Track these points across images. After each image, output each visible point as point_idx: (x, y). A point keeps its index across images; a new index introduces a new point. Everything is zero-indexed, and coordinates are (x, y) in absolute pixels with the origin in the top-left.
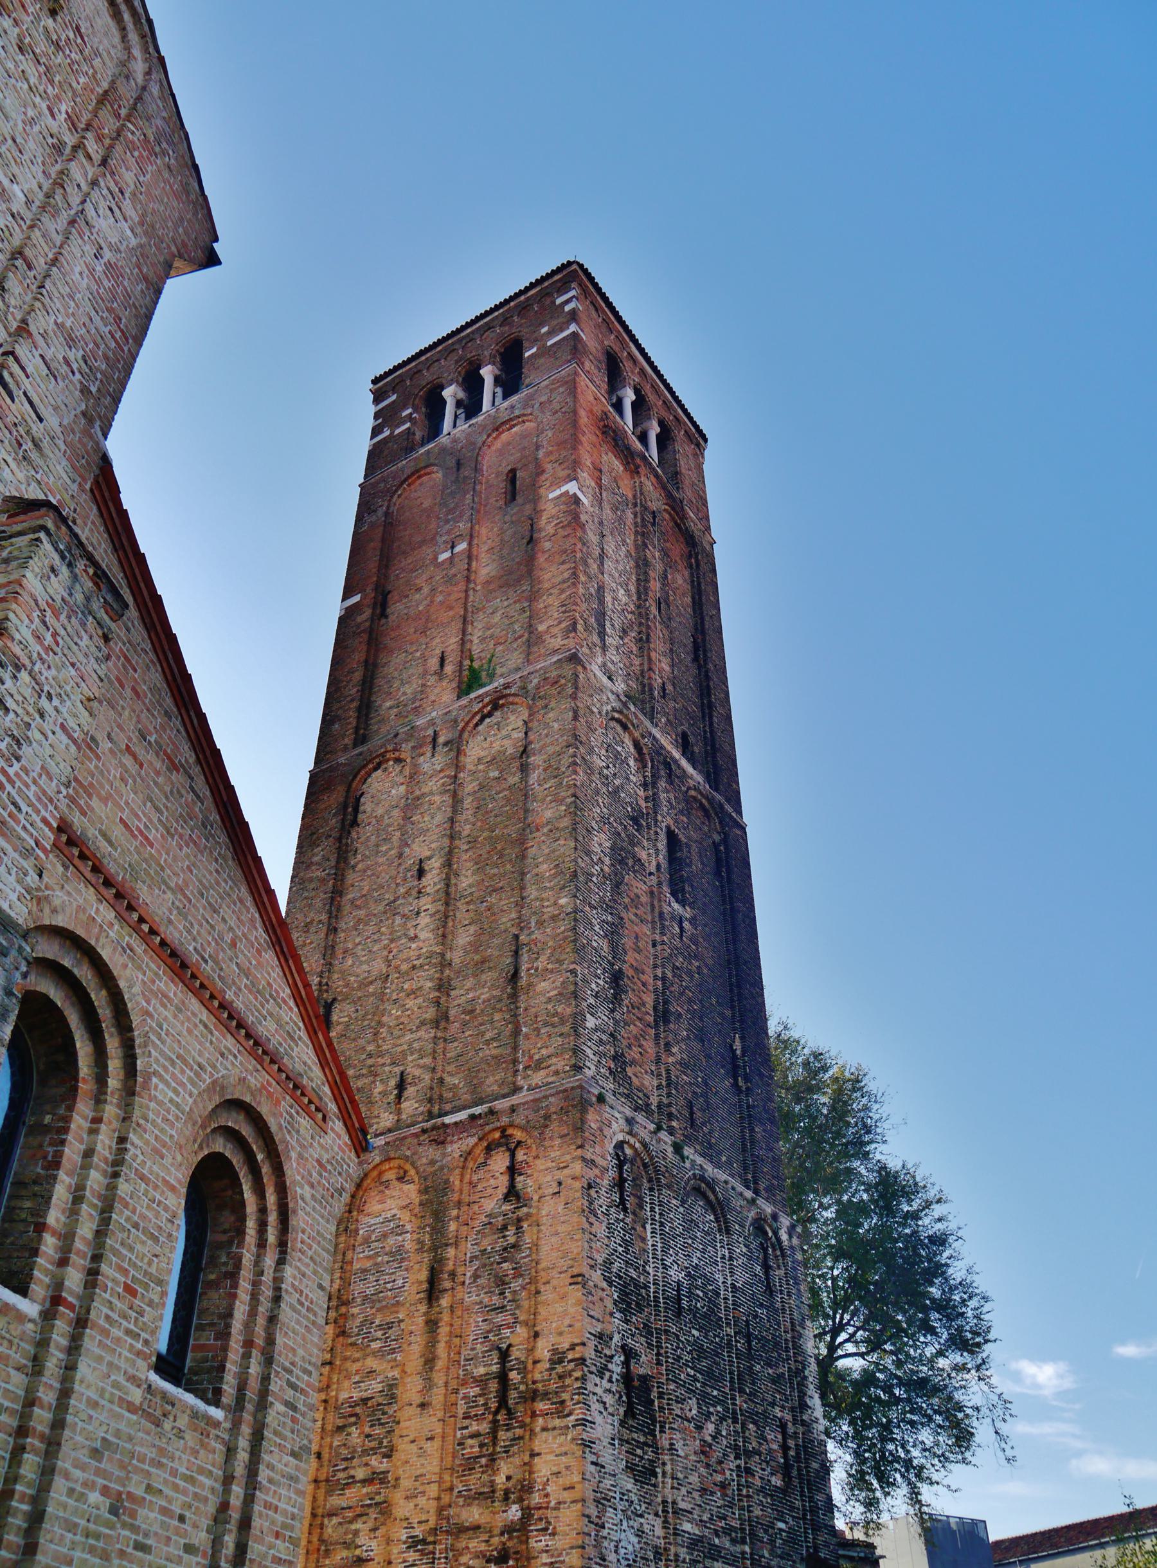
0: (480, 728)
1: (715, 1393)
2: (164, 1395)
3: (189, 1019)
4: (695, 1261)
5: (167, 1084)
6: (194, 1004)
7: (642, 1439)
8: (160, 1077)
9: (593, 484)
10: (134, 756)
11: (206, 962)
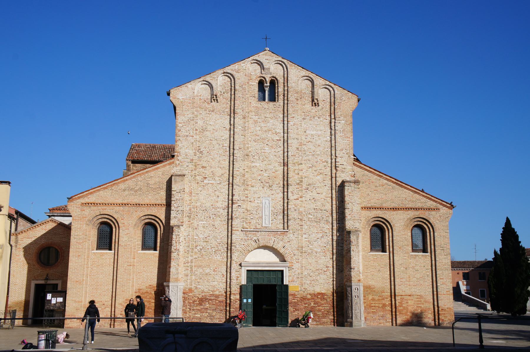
2: (415, 255)
3: (399, 214)
5: (398, 224)
6: (400, 212)
8: (396, 224)
10: (376, 190)
11: (400, 205)
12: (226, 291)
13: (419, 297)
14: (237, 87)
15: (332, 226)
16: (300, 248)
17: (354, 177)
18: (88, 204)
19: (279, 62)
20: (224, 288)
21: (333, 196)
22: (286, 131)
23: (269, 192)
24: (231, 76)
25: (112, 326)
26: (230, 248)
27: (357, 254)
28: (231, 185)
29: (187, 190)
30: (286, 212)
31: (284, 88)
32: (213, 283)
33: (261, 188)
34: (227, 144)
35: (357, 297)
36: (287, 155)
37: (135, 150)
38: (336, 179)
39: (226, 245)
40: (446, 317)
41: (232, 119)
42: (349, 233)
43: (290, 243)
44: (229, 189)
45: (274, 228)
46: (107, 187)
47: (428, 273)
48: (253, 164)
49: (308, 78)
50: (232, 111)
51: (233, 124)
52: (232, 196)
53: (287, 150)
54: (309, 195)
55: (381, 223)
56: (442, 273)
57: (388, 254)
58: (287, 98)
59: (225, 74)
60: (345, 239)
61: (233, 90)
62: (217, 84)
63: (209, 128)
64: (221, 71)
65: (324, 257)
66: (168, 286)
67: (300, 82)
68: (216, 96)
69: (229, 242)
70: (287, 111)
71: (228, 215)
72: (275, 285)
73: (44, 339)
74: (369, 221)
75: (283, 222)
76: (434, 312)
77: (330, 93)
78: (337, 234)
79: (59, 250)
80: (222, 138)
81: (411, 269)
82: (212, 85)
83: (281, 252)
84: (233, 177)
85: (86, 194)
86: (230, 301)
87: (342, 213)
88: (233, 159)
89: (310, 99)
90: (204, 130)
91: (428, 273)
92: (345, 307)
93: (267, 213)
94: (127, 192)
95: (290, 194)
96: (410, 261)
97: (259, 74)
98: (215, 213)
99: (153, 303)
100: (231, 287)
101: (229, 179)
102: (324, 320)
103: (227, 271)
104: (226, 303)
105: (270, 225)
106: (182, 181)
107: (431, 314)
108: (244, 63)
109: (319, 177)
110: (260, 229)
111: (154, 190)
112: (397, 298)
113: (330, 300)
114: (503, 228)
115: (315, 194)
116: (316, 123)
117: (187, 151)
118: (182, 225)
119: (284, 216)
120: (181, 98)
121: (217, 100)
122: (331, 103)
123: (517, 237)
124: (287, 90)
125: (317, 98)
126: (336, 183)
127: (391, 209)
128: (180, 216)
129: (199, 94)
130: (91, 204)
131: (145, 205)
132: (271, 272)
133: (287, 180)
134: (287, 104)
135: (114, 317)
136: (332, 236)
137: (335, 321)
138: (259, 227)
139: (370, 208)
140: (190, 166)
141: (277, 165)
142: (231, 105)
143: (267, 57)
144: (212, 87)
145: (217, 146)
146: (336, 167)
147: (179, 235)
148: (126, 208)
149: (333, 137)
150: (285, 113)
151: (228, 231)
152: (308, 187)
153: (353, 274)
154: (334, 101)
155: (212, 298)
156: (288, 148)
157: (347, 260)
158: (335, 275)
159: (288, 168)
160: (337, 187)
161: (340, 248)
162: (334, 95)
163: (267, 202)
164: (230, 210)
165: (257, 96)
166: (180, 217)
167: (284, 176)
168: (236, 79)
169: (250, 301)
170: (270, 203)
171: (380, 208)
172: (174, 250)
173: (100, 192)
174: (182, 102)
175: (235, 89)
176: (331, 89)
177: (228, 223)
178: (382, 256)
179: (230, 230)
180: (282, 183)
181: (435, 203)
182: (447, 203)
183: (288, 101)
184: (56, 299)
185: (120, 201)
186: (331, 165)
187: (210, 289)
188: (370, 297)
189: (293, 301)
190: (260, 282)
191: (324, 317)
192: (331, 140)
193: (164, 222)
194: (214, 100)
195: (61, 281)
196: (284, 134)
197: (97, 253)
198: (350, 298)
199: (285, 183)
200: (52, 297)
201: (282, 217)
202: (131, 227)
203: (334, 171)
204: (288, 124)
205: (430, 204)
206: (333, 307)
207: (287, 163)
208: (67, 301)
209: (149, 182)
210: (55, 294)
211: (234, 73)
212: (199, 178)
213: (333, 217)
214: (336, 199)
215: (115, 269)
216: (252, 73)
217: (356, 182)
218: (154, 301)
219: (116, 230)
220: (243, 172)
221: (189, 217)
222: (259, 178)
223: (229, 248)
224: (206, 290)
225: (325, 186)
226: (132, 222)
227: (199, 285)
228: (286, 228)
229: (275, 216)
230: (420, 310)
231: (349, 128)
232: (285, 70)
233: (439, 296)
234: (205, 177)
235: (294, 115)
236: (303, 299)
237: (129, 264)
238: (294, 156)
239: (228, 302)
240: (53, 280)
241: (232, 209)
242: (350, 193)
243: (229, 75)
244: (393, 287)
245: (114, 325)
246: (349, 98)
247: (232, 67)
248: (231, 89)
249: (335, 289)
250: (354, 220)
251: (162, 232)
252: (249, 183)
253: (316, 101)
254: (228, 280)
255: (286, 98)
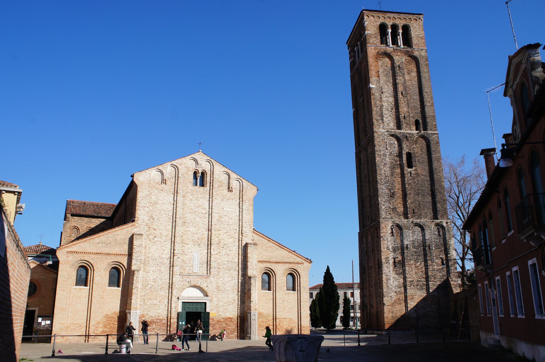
0: (369, 145)
1: (420, 258)
4: (415, 238)
7: (399, 269)
9: (376, 78)
12: (168, 316)
13: (289, 319)
14: (180, 175)
15: (239, 273)
16: (218, 287)
17: (253, 241)
18: (72, 252)
19: (208, 160)
20: (166, 315)
21: (240, 253)
22: (211, 208)
23: (198, 249)
24: (176, 168)
25: (87, 342)
26: (171, 286)
27: (255, 292)
28: (173, 243)
29: (143, 245)
30: (209, 263)
31: (211, 178)
32: (159, 311)
33: (193, 246)
34: (171, 214)
35: (254, 320)
36: (211, 223)
37: (71, 205)
38: (242, 242)
39: (168, 284)
40: (305, 331)
41: (175, 197)
42: (250, 278)
43: (211, 284)
44: (171, 245)
45: (200, 273)
46: (86, 240)
47: (295, 304)
48: (188, 229)
49: (227, 173)
50: (176, 191)
51: (176, 201)
52: (174, 251)
53: (211, 220)
54: (223, 252)
55: (269, 272)
56: (304, 304)
57: (272, 292)
58: (213, 185)
59: (172, 166)
60: (246, 281)
61: (177, 177)
62: (166, 172)
63: (160, 202)
64: (170, 163)
65: (232, 294)
66: (130, 313)
67: (221, 175)
68: (165, 180)
69: (171, 282)
70: (212, 194)
71: (170, 263)
72: (201, 313)
73: (125, 347)
74: (262, 270)
75: (206, 270)
76: (298, 329)
77: (240, 184)
78: (241, 278)
79: (37, 284)
80: (169, 210)
81: (286, 302)
82: (163, 172)
83: (205, 290)
84: (175, 237)
85: (71, 245)
86: (170, 323)
87: (245, 264)
88: (175, 225)
89: (227, 187)
90: (156, 203)
91: (295, 304)
92: (245, 327)
93: (197, 263)
94: (100, 245)
95: (212, 251)
96: (285, 296)
97: (194, 168)
98: (161, 262)
99: (116, 324)
100: (171, 313)
101: (172, 238)
102: (231, 335)
103: (168, 303)
104: (167, 324)
105: (198, 272)
106: (141, 239)
107: (296, 330)
108: (185, 159)
109: (231, 240)
110: (191, 274)
111: (120, 244)
112: (277, 320)
113: (235, 322)
114: (325, 273)
115: (228, 251)
116: (230, 203)
117: (144, 217)
118: (140, 270)
119: (207, 265)
120: (141, 180)
121: (166, 183)
122: (240, 191)
123: (333, 278)
124: (213, 180)
125: (231, 186)
126: (242, 244)
127: (275, 262)
128: (138, 263)
129: (154, 178)
130: (74, 252)
131: (113, 254)
132: (190, 303)
133: (211, 241)
134: (212, 189)
135: (88, 335)
136: (238, 279)
137: (239, 336)
138: (191, 272)
139: (262, 262)
140: (146, 228)
141: (204, 230)
142: (175, 187)
143: (200, 157)
144: (163, 174)
145: (164, 215)
146: (242, 233)
147: (138, 277)
148: (100, 256)
149: (241, 213)
150: (211, 195)
151: (170, 275)
152: (224, 246)
153: (252, 305)
154: (242, 189)
155: (158, 321)
156: (211, 219)
157: (248, 296)
158: (239, 306)
159: (211, 233)
160: (242, 247)
161: (243, 288)
162: (243, 185)
163: (197, 255)
164: (172, 260)
165: (192, 182)
166: (139, 264)
167: (208, 238)
168: (179, 170)
169: (184, 323)
170: (199, 256)
171: (269, 262)
172: (134, 287)
173: (81, 244)
174: (142, 183)
175: (178, 177)
176: (241, 181)
177: (170, 269)
178: (269, 293)
179: (171, 274)
180: (207, 243)
181: (301, 260)
182: (305, 258)
183: (213, 187)
184: (45, 322)
185: (95, 251)
186: (239, 232)
187: (157, 315)
188: (261, 320)
189: (212, 323)
190: (191, 310)
191: (231, 333)
192: (239, 215)
193: (126, 267)
194: (164, 183)
195: (38, 308)
196: (209, 209)
197: (76, 288)
198: (249, 321)
199: (209, 243)
200: (42, 320)
201: (206, 266)
202: (103, 270)
203: (241, 236)
204: (212, 203)
205: (299, 260)
206: (238, 327)
207: (211, 229)
208: (53, 323)
209: (117, 238)
210: (44, 318)
211: (178, 165)
212: (151, 237)
213: (239, 267)
214: (241, 255)
215: (90, 300)
216: (190, 166)
217: (255, 244)
218: (117, 323)
219: (91, 272)
220: (181, 234)
221: (144, 264)
222: (192, 238)
223: (170, 286)
224: (154, 315)
225: (235, 246)
226: (103, 266)
227: (149, 312)
228: (209, 273)
229: (201, 265)
230: (290, 328)
231: (251, 208)
232: (212, 166)
233: (302, 318)
234: (155, 236)
235: (216, 197)
236: (219, 321)
237: (100, 297)
238: (216, 224)
239: (169, 324)
240: (32, 307)
241: (173, 259)
242: (251, 251)
243: (175, 166)
244: (275, 313)
245: (88, 340)
246: (252, 189)
247: (177, 161)
248: (175, 176)
249: (239, 315)
250: (253, 269)
251: (124, 274)
252: (185, 242)
253: (231, 188)
254: (169, 309)
255: (211, 185)
